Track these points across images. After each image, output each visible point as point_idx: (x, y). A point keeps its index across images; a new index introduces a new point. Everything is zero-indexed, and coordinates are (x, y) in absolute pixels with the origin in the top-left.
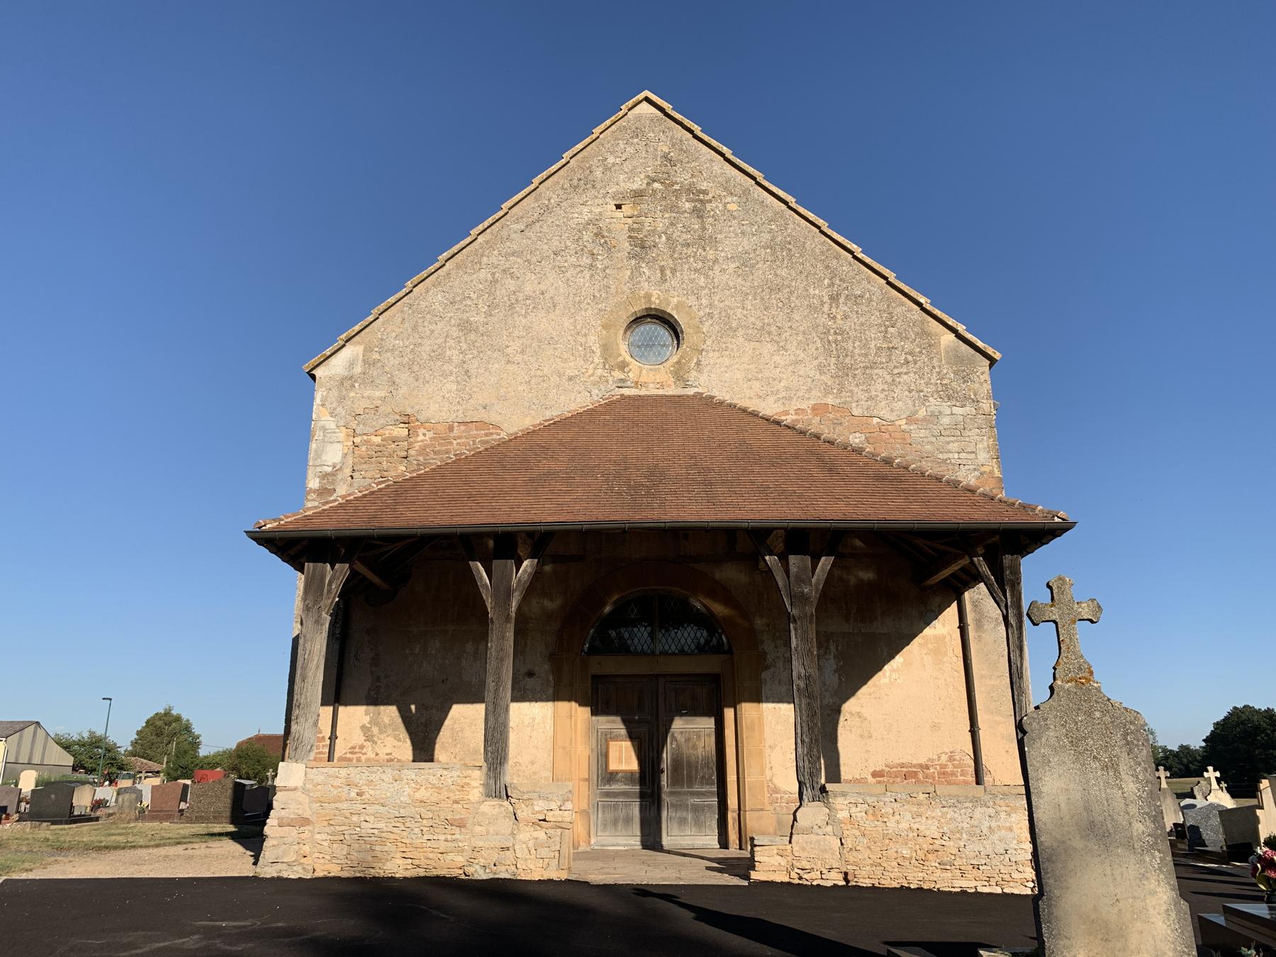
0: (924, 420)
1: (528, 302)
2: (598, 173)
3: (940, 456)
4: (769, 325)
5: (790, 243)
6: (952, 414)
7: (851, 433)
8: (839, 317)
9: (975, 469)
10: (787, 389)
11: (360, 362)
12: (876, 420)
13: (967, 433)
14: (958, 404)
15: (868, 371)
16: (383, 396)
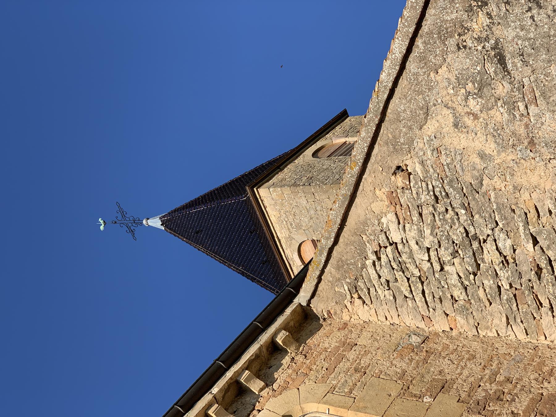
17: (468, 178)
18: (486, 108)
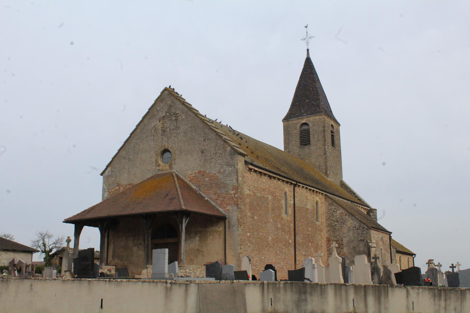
0: (222, 172)
1: (141, 151)
2: (155, 113)
3: (225, 182)
4: (190, 150)
5: (195, 126)
6: (229, 170)
7: (206, 178)
8: (205, 145)
9: (232, 185)
10: (193, 167)
11: (110, 172)
12: (212, 174)
13: (232, 175)
14: (230, 167)
15: (211, 160)
16: (114, 179)
17: (345, 223)
18: (353, 227)
